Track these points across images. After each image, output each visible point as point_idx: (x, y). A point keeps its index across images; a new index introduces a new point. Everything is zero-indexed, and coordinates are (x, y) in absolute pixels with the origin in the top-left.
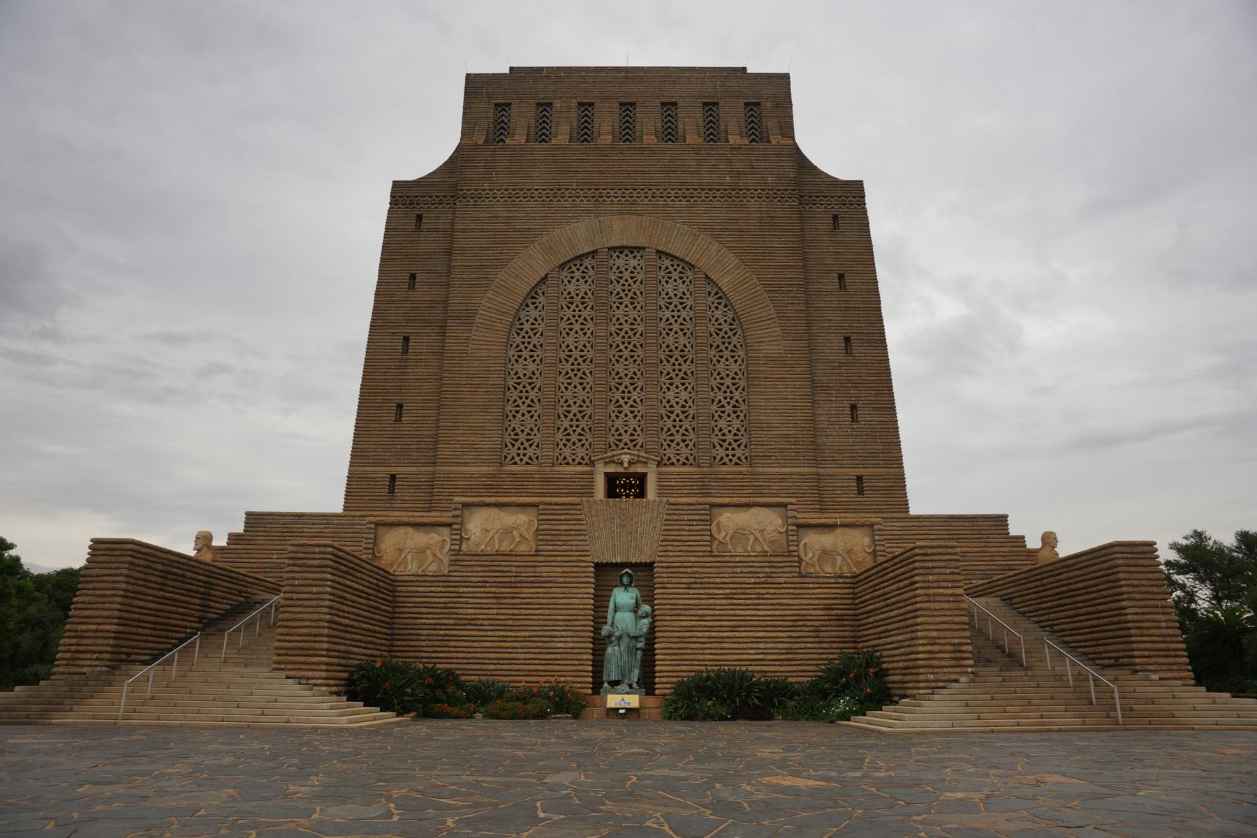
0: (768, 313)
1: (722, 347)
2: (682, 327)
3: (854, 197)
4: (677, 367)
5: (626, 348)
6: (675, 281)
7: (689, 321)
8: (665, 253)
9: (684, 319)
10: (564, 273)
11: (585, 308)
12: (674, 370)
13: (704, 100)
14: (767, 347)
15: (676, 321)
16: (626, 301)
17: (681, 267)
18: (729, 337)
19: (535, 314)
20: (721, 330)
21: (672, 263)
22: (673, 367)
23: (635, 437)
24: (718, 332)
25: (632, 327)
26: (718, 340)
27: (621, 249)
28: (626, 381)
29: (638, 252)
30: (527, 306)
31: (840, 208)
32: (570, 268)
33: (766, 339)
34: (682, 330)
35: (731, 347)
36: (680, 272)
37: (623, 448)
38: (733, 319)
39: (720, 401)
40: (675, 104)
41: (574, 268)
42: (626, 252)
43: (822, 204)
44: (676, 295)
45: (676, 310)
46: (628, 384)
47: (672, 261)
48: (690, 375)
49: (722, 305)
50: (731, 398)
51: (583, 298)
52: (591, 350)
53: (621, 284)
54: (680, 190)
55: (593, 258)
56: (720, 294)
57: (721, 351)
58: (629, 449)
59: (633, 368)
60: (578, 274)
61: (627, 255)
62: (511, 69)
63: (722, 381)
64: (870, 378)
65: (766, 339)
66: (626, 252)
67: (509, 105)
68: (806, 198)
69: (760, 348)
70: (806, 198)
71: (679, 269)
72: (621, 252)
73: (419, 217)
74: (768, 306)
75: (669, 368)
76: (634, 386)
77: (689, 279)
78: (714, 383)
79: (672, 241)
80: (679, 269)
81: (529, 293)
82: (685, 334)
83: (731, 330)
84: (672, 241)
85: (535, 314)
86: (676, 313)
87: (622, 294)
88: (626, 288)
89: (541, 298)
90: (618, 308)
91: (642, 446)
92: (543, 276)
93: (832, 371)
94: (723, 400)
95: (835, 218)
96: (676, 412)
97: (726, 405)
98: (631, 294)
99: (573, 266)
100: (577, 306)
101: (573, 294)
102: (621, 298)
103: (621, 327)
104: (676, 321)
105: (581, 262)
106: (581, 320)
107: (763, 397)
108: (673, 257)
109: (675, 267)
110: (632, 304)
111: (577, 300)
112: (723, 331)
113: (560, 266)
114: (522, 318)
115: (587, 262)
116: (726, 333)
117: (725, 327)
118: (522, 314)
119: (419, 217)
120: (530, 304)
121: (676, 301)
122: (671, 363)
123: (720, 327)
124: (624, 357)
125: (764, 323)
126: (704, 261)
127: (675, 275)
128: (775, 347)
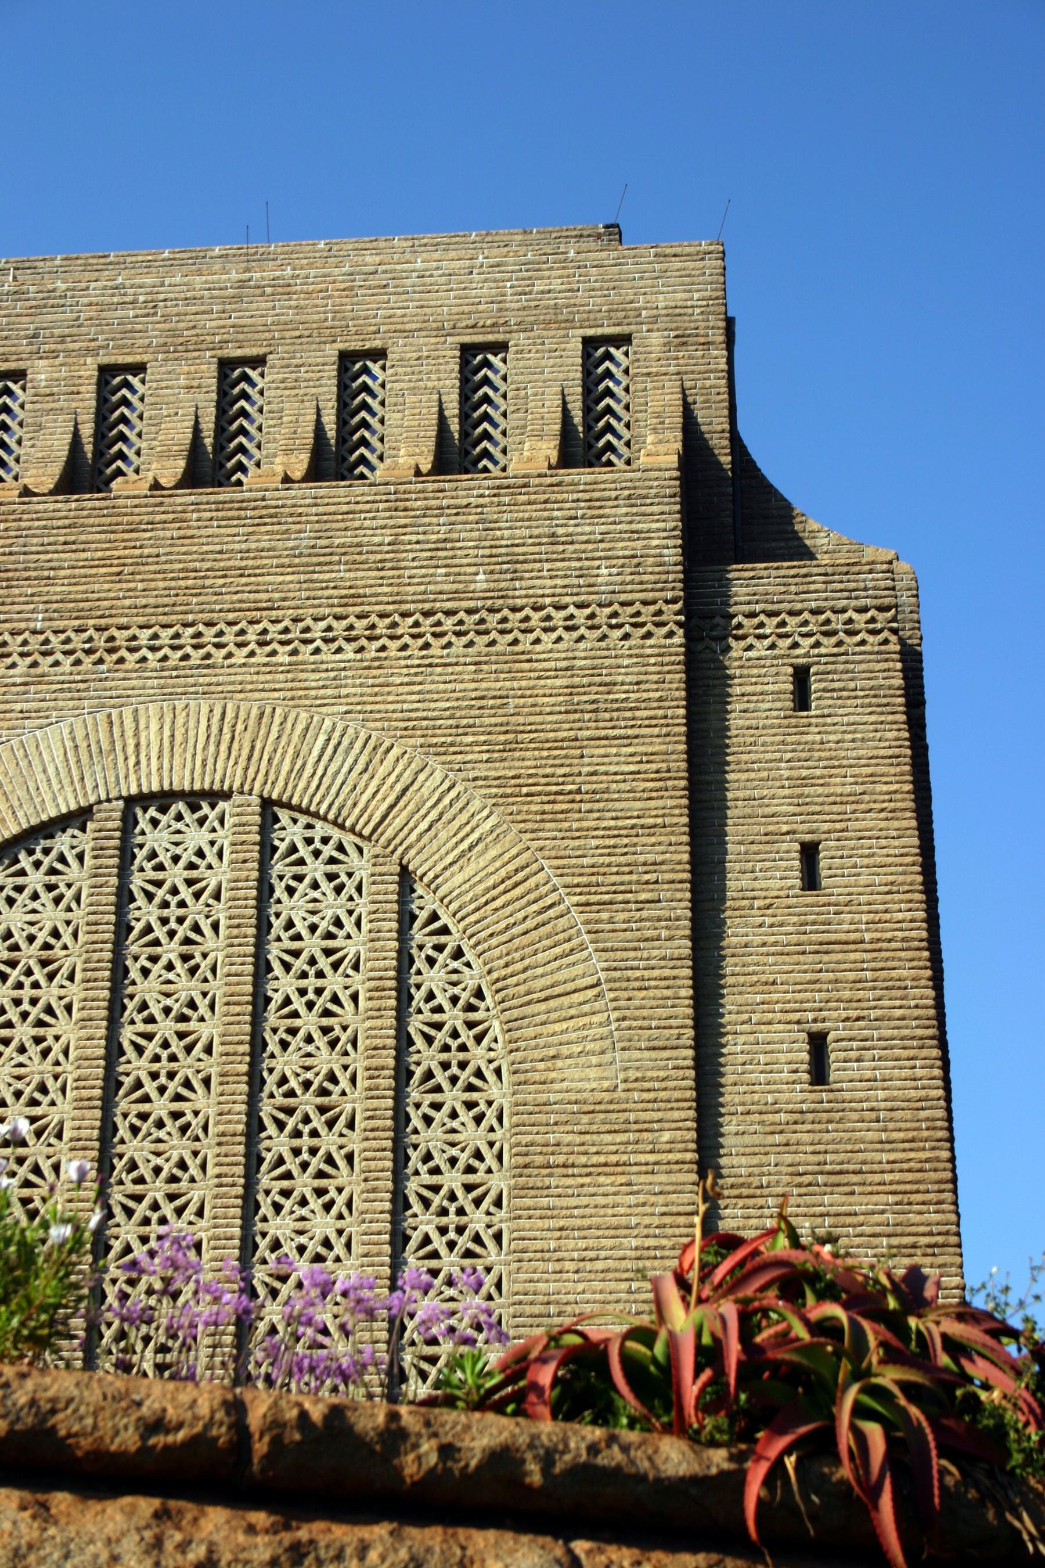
0: (579, 969)
2: (326, 1022)
3: (864, 610)
4: (306, 1142)
5: (162, 1090)
9: (335, 999)
12: (296, 1152)
13: (467, 339)
14: (577, 1073)
15: (310, 1005)
16: (171, 951)
20: (438, 1026)
21: (309, 833)
22: (296, 1143)
24: (432, 1032)
25: (182, 1027)
27: (163, 799)
28: (157, 1190)
29: (213, 806)
33: (565, 1050)
34: (326, 1030)
35: (465, 1076)
41: (25, 862)
43: (759, 637)
45: (312, 972)
46: (160, 1197)
47: (309, 826)
48: (341, 1163)
49: (447, 951)
50: (460, 1230)
51: (47, 946)
52: (59, 1100)
53: (157, 900)
55: (83, 830)
59: (178, 1147)
60: (35, 880)
61: (179, 817)
63: (435, 1180)
64: (885, 1157)
65: (565, 1050)
66: (181, 806)
68: (718, 620)
69: (553, 1075)
70: (718, 620)
72: (164, 810)
74: (582, 947)
76: (178, 1202)
77: (356, 878)
83: (470, 1025)
86: (311, 983)
93: (770, 1139)
94: (434, 1235)
95: (801, 676)
97: (443, 1251)
100: (29, 972)
102: (157, 943)
103: (150, 1028)
104: (310, 1005)
105: (48, 843)
107: (552, 1223)
115: (62, 843)
116: (455, 1035)
117: (454, 1017)
123: (437, 1017)
125: (566, 1000)
126: (398, 822)
128: (592, 1073)
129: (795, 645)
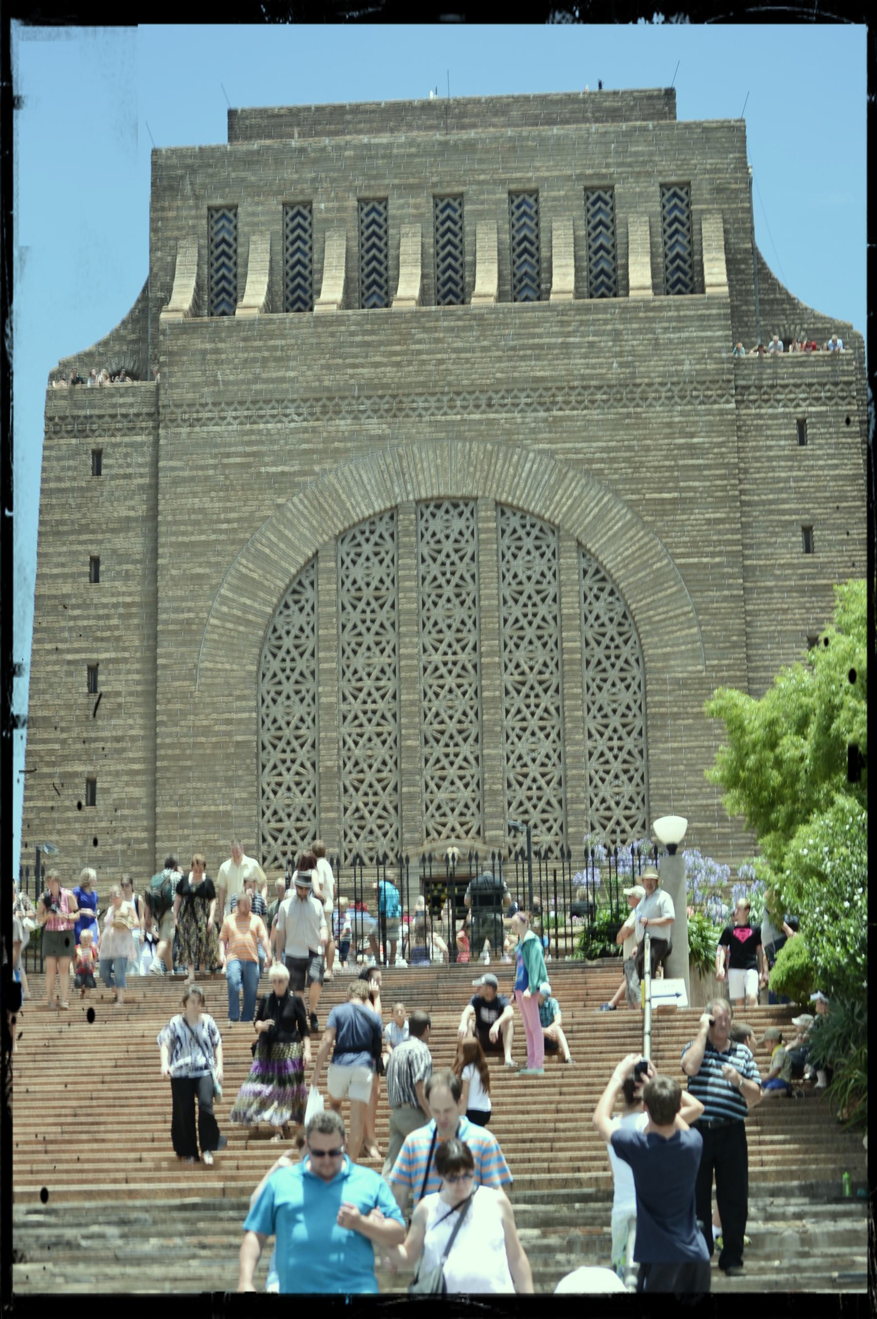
1: (606, 664)
2: (540, 632)
6: (529, 553)
7: (552, 622)
8: (511, 506)
9: (544, 619)
10: (345, 547)
11: (382, 606)
15: (530, 623)
16: (449, 591)
17: (537, 528)
18: (617, 647)
19: (299, 619)
23: (467, 819)
26: (599, 653)
30: (287, 606)
31: (811, 405)
32: (354, 537)
36: (537, 538)
37: (448, 837)
38: (624, 616)
39: (602, 755)
40: (534, 193)
41: (360, 539)
42: (446, 505)
43: (778, 401)
44: (529, 578)
54: (534, 390)
56: (601, 576)
57: (604, 670)
58: (458, 837)
60: (367, 549)
61: (447, 512)
62: (232, 114)
66: (446, 505)
67: (233, 208)
71: (535, 532)
72: (438, 507)
73: (98, 455)
75: (519, 702)
78: (592, 725)
79: (522, 485)
80: (535, 532)
81: (288, 587)
82: (545, 645)
84: (522, 485)
85: (299, 619)
86: (530, 610)
87: (442, 580)
88: (448, 568)
89: (309, 593)
90: (435, 604)
91: (478, 832)
92: (310, 554)
95: (801, 425)
96: (531, 776)
97: (612, 759)
98: (455, 580)
99: (358, 535)
101: (361, 583)
106: (375, 627)
108: (524, 513)
109: (528, 528)
110: (458, 595)
111: (368, 594)
112: (608, 636)
113: (336, 538)
114: (279, 627)
117: (611, 630)
118: (279, 621)
119: (98, 455)
120: (291, 603)
121: (529, 588)
122: (522, 694)
124: (447, 688)
127: (528, 543)
129: (798, 405)
